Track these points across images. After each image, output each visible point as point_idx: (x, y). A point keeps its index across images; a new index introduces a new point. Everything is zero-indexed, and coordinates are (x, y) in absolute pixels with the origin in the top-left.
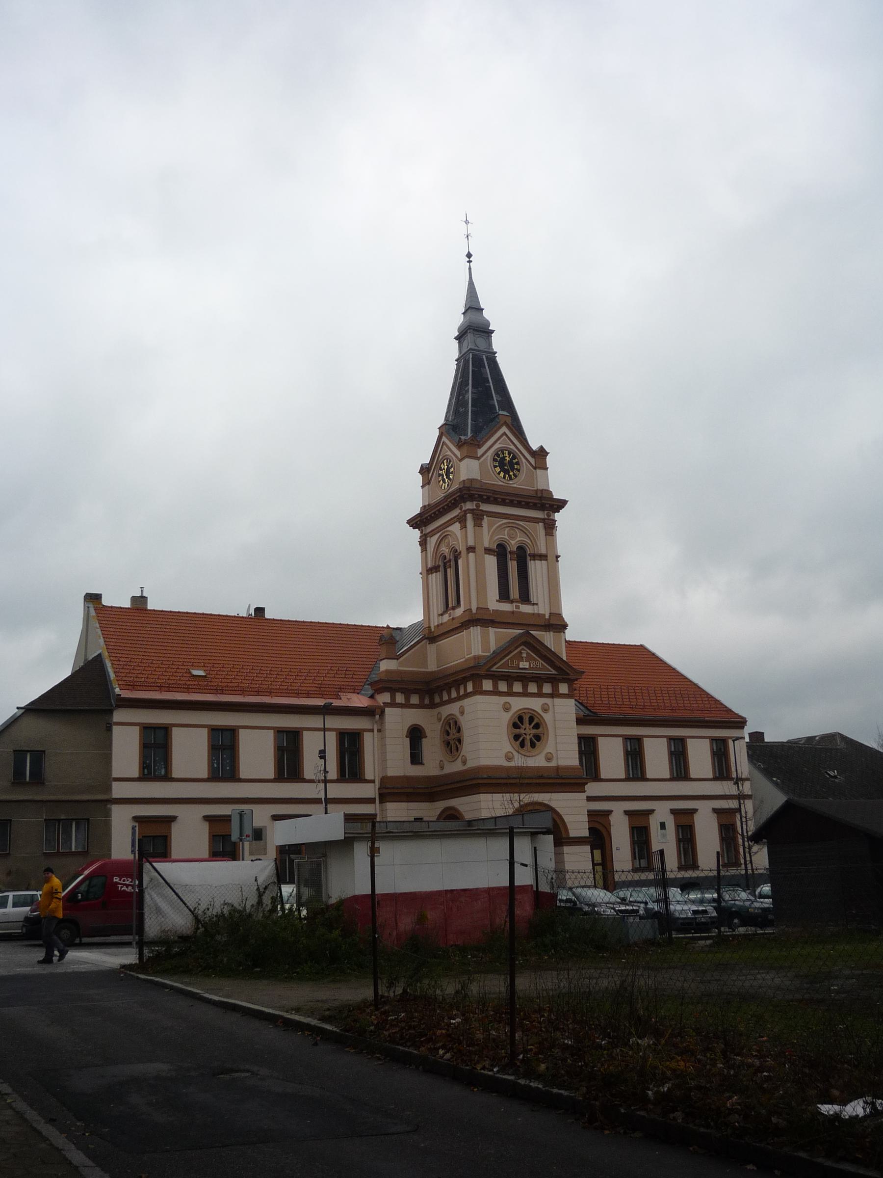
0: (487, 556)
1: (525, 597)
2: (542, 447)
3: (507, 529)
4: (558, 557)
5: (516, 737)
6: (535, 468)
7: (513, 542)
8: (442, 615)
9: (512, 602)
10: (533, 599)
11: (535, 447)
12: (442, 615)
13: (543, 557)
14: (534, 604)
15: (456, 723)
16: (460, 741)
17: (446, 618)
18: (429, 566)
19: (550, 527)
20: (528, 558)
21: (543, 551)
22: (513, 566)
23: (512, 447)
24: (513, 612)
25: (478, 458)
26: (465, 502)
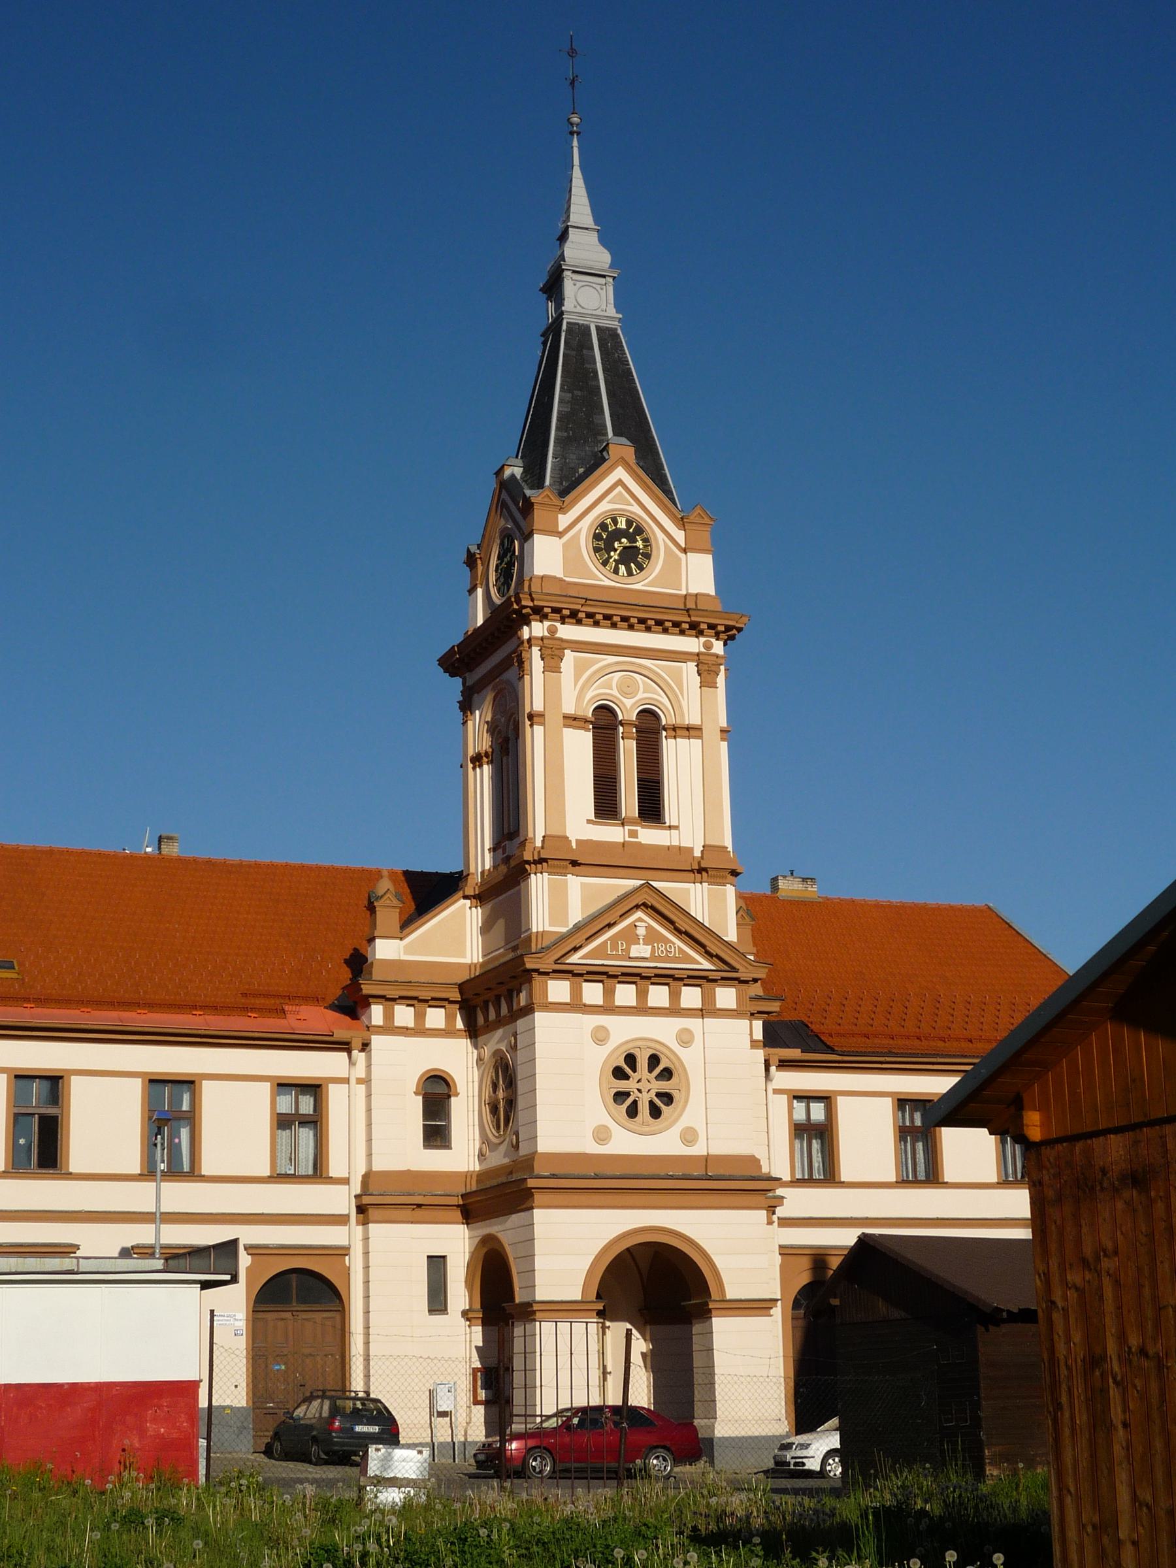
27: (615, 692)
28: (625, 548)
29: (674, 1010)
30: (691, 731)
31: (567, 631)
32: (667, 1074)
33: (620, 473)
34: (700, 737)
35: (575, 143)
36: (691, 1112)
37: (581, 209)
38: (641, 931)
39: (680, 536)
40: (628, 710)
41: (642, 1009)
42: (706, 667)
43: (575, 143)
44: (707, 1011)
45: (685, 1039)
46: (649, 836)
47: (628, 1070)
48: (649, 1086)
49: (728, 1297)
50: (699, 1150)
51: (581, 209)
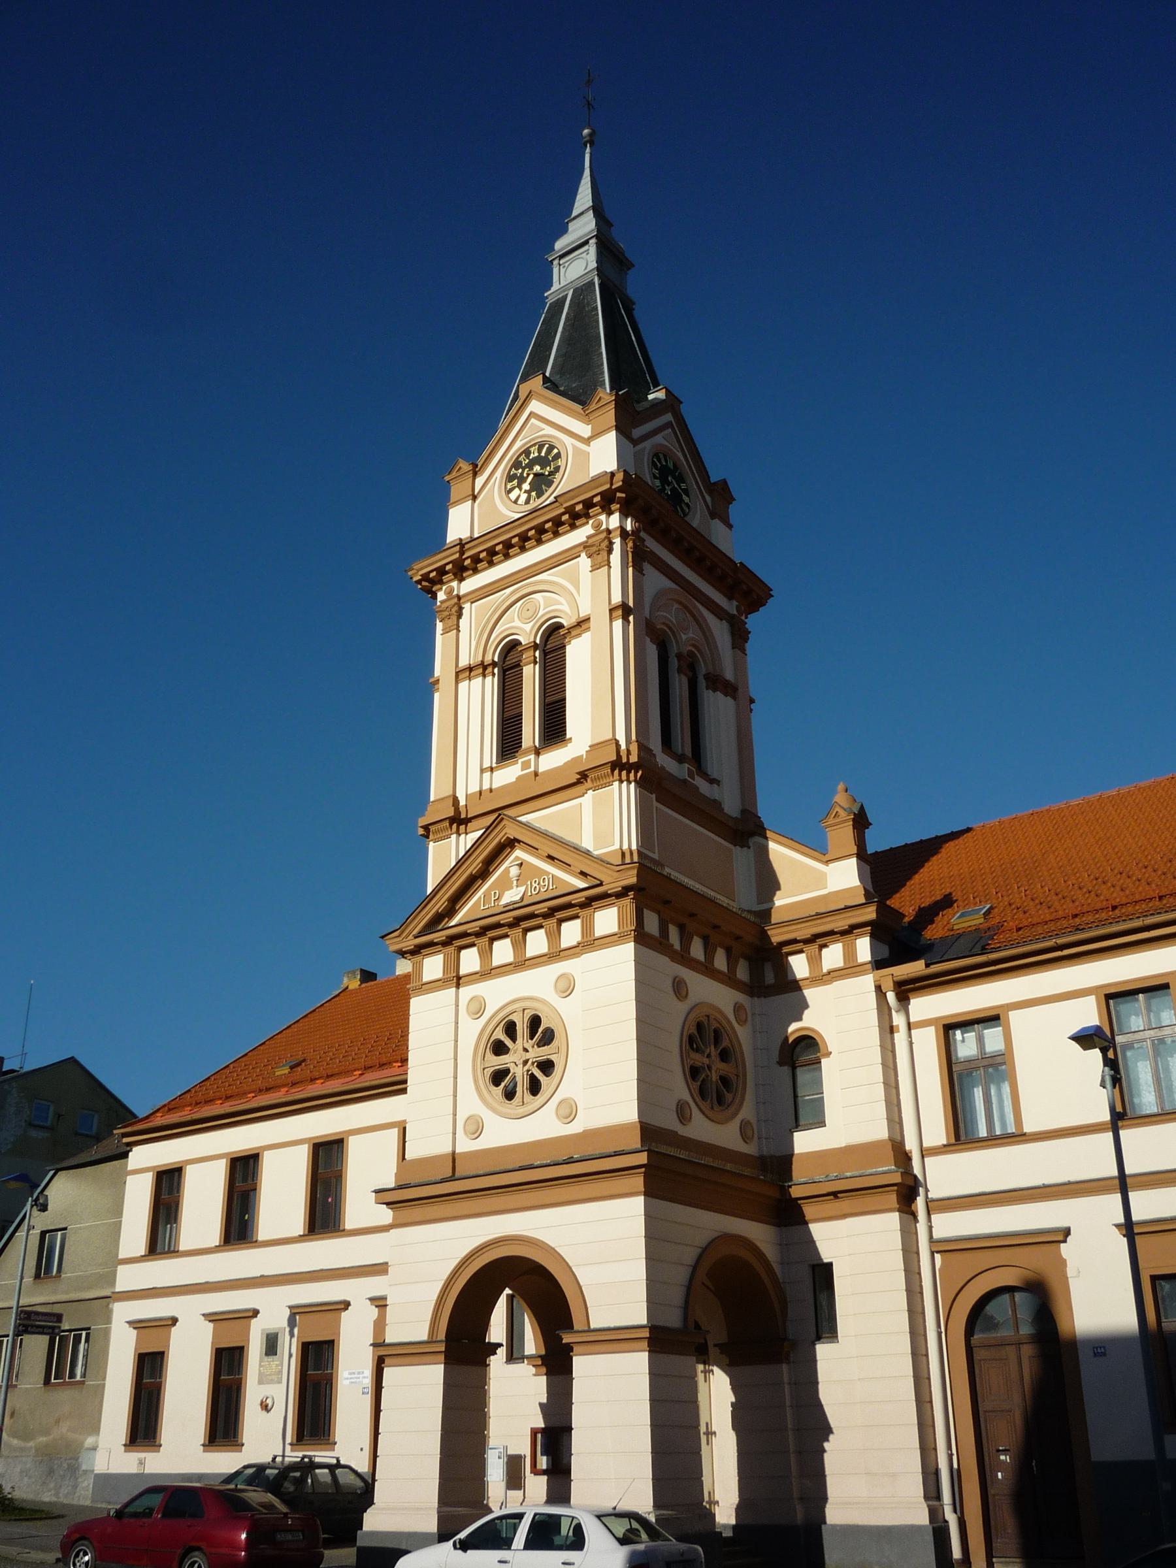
0: (648, 640)
1: (697, 757)
2: (724, 482)
3: (676, 606)
4: (752, 701)
5: (694, 1072)
6: (713, 515)
7: (684, 637)
8: (492, 769)
9: (681, 759)
10: (713, 771)
11: (714, 479)
12: (492, 769)
13: (730, 689)
14: (713, 781)
15: (535, 1022)
16: (547, 1067)
17: (510, 774)
18: (464, 662)
19: (740, 636)
20: (702, 683)
21: (729, 675)
22: (679, 685)
23: (680, 455)
24: (685, 781)
25: (635, 443)
26: (610, 513)
27: (517, 623)
28: (536, 475)
29: (555, 954)
30: (582, 624)
31: (472, 583)
32: (548, 1037)
33: (535, 406)
34: (588, 629)
35: (588, 150)
36: (571, 1082)
37: (584, 197)
38: (514, 871)
39: (585, 430)
40: (527, 632)
41: (521, 964)
42: (598, 550)
43: (588, 150)
44: (590, 943)
45: (567, 987)
46: (553, 759)
47: (508, 1042)
48: (528, 1056)
49: (592, 1327)
50: (576, 1127)
51: (584, 197)
